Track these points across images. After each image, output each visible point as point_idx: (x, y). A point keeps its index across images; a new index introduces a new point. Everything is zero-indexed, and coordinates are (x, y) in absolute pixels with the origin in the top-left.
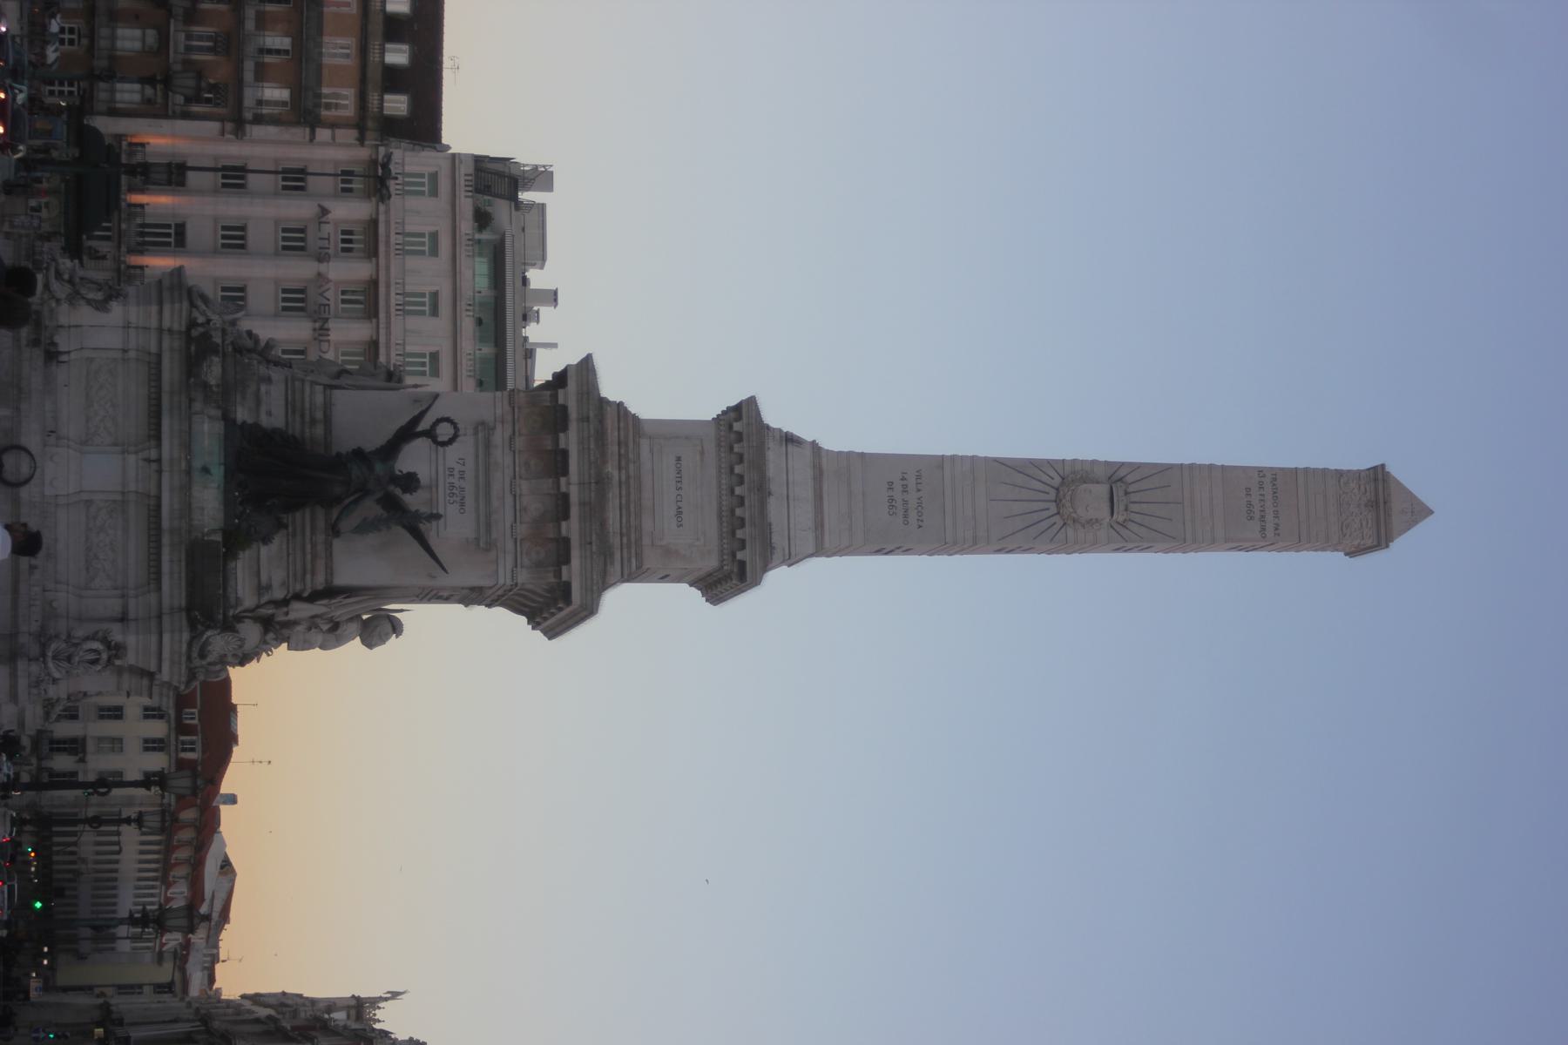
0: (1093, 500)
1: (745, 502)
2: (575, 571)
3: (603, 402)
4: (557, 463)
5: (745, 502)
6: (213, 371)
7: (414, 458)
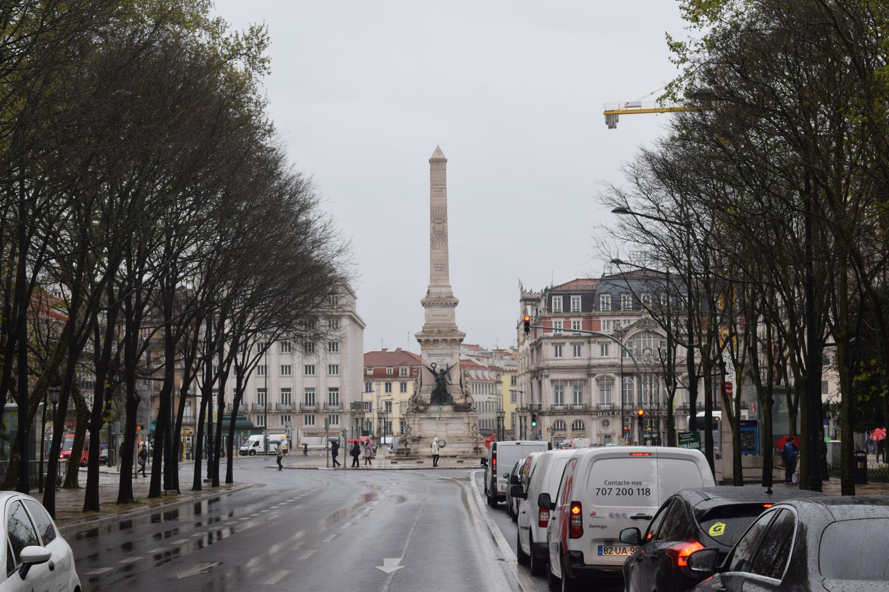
0: (439, 227)
2: (457, 338)
4: (436, 341)
6: (422, 408)
7: (438, 370)
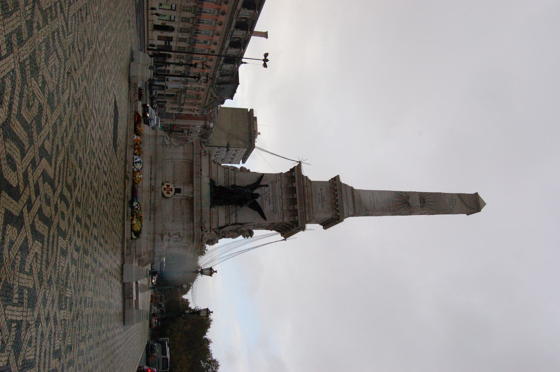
1: (335, 203)
2: (299, 218)
3: (303, 176)
4: (292, 190)
5: (335, 203)
